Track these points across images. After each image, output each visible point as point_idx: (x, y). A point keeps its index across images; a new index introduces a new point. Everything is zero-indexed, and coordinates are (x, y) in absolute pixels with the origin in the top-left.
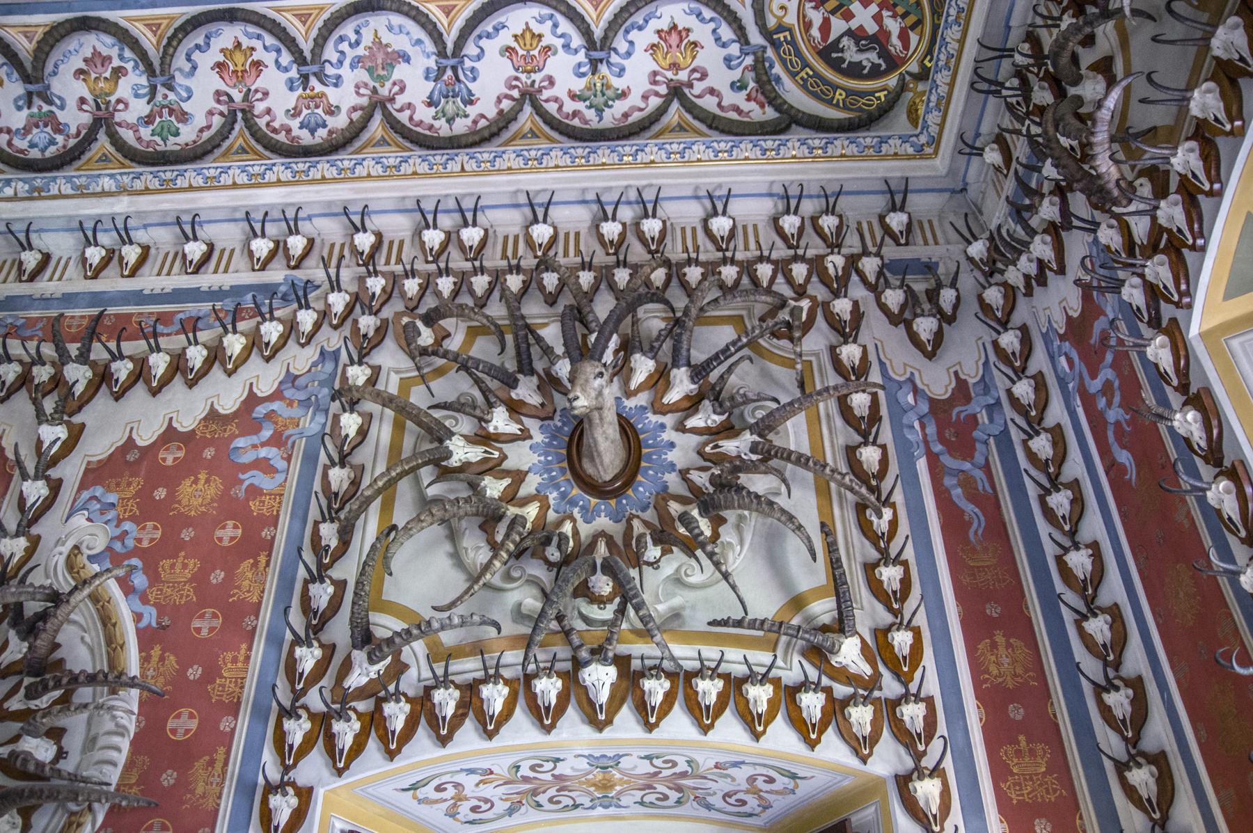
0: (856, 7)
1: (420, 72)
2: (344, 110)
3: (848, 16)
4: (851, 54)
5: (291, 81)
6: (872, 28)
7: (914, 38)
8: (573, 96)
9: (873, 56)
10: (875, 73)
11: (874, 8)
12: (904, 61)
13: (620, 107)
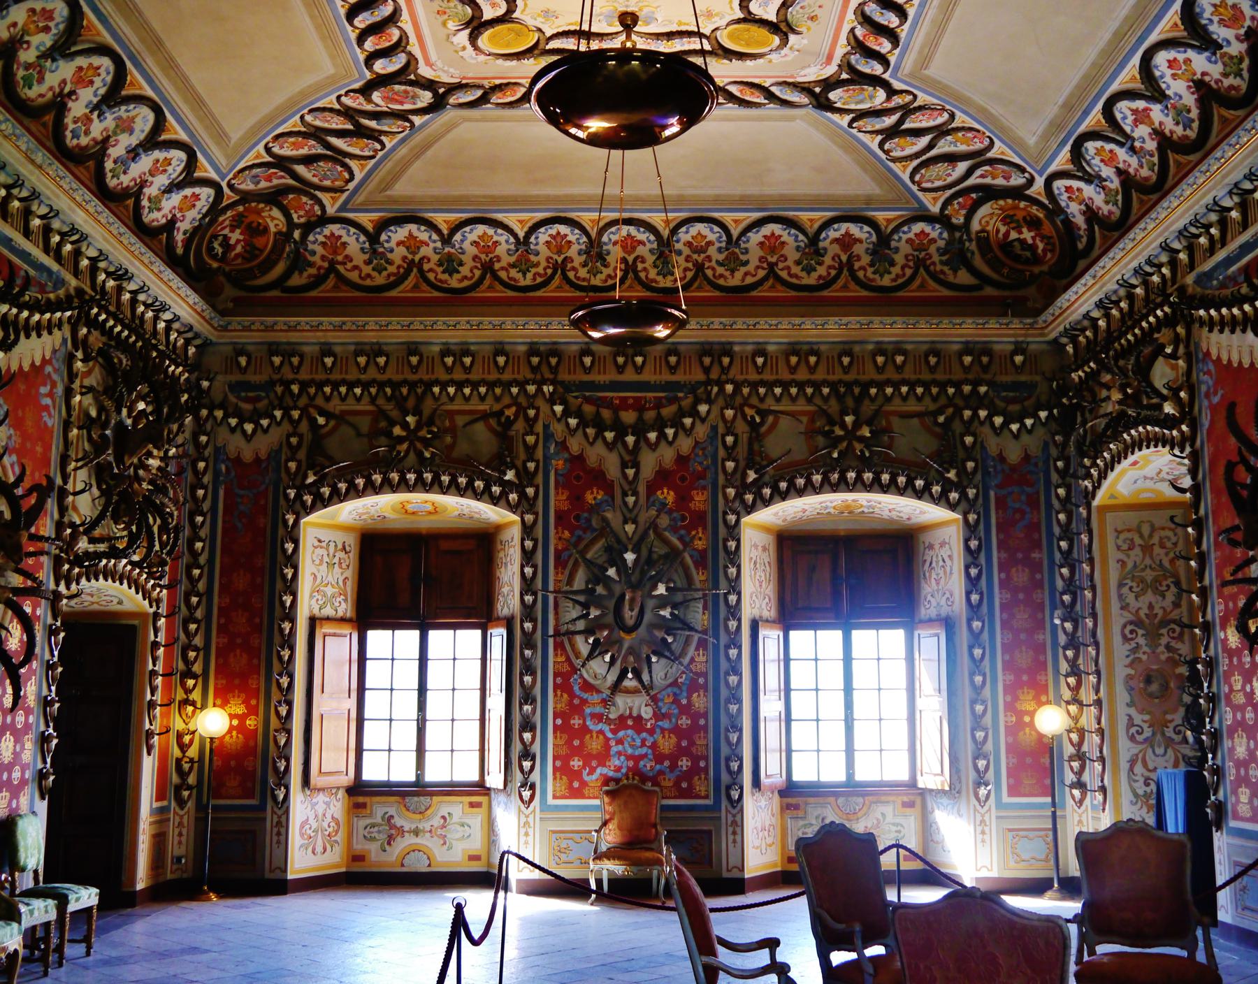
0: (238, 231)
1: (127, 144)
2: (92, 135)
3: (232, 231)
4: (216, 245)
5: (91, 102)
6: (232, 242)
7: (239, 261)
8: (149, 199)
9: (220, 251)
10: (214, 257)
11: (241, 237)
12: (228, 264)
13: (156, 215)
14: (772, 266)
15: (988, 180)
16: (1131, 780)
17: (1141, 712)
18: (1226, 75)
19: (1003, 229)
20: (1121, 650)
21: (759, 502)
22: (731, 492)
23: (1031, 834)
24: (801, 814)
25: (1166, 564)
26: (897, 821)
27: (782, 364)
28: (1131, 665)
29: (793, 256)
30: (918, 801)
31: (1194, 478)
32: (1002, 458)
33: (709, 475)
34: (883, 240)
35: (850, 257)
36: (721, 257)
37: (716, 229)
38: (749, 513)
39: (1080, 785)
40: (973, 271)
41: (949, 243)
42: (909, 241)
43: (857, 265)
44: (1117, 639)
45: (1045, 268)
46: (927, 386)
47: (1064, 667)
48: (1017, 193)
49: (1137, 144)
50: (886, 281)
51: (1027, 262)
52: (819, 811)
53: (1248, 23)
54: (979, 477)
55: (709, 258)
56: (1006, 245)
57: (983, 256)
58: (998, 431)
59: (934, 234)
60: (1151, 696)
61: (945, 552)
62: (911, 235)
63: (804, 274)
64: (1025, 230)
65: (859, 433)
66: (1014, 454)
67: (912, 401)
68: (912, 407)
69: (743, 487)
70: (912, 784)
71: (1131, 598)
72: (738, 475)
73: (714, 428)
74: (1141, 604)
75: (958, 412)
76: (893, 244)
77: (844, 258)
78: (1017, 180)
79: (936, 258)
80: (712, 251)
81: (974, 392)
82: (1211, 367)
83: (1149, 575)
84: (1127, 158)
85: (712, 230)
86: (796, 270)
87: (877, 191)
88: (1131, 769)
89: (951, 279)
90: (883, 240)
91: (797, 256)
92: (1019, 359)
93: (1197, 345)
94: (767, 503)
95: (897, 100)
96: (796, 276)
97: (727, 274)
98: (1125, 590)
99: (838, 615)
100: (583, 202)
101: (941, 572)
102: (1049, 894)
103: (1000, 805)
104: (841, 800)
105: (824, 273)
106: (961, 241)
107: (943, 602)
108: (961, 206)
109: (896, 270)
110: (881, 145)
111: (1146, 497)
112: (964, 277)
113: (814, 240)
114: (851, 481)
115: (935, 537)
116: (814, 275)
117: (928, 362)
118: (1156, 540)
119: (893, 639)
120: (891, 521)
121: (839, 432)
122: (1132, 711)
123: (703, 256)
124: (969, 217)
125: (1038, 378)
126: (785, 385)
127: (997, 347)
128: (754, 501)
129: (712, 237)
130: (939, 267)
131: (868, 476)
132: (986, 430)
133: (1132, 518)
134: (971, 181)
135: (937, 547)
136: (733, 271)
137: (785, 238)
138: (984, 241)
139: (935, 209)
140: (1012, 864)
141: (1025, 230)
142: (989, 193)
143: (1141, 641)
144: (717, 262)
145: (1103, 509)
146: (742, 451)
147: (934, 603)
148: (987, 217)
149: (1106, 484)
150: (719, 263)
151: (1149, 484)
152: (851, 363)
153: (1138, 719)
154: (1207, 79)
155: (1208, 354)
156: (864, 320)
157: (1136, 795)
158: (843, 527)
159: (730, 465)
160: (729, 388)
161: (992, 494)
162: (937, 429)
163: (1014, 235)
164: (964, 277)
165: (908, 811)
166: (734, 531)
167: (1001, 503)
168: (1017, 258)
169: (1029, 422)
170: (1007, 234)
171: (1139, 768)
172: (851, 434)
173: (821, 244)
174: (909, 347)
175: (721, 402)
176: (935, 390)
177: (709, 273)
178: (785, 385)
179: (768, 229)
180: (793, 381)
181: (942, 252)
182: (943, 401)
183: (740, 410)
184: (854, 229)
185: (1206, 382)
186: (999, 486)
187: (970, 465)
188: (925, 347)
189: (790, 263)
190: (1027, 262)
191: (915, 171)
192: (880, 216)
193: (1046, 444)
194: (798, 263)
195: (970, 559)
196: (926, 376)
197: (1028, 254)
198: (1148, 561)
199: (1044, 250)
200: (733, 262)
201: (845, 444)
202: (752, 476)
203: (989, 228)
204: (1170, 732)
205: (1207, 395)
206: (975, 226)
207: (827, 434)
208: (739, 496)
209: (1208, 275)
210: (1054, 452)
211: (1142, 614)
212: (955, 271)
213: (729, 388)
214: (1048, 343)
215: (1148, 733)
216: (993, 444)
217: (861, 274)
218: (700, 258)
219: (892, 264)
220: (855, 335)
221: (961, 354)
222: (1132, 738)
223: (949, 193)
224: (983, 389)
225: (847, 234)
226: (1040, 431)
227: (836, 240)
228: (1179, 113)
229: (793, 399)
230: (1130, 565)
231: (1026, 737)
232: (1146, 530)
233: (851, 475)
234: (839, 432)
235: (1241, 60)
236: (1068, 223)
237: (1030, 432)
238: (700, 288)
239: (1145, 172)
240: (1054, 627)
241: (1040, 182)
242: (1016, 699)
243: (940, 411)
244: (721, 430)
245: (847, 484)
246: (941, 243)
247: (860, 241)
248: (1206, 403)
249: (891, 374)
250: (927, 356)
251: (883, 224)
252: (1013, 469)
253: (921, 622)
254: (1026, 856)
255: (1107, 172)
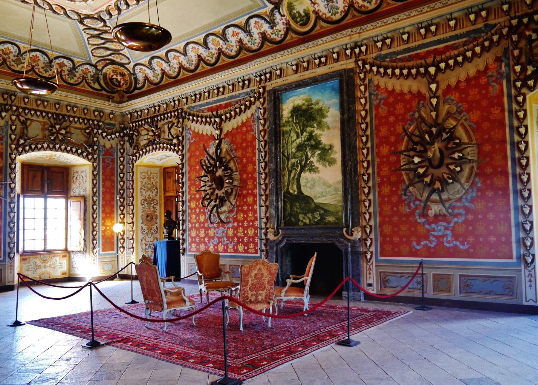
14: (33, 66)
15: (114, 59)
16: (141, 245)
17: (145, 225)
18: (208, 56)
19: (112, 74)
20: (140, 207)
21: (23, 152)
22: (13, 146)
23: (108, 263)
24: (27, 261)
25: (154, 183)
26: (61, 262)
27: (34, 103)
28: (143, 212)
29: (41, 64)
30: (68, 255)
31: (182, 161)
32: (104, 146)
33: (5, 139)
34: (74, 68)
35: (61, 70)
36: (14, 58)
37: (16, 48)
38: (20, 155)
39: (123, 247)
40: (100, 85)
41: (95, 74)
42: (82, 70)
43: (63, 74)
44: (139, 204)
45: (122, 89)
46: (84, 119)
47: (119, 212)
48: (122, 65)
49: (171, 64)
50: (72, 81)
51: (117, 86)
52: (34, 260)
53: (220, 46)
54: (97, 152)
55: (9, 58)
56: (111, 79)
57: (104, 80)
58: (103, 138)
59: (91, 70)
60: (148, 221)
61: (83, 175)
62: (83, 69)
63: (44, 72)
64: (119, 76)
65: (61, 132)
66: (108, 146)
67: (78, 123)
68: (78, 125)
69: (18, 145)
70: (66, 250)
71: (144, 193)
72: (16, 140)
73: (7, 122)
74: (147, 194)
75: (93, 130)
76: (77, 70)
77: (59, 70)
78: (125, 61)
79: (89, 78)
80: (11, 55)
81: (98, 124)
82: (191, 132)
83: (149, 186)
84: (166, 67)
85: (13, 48)
86: (42, 70)
87: (78, 52)
88: (142, 242)
89: (93, 85)
90: (74, 68)
91: (43, 65)
92: (111, 116)
93: (186, 126)
94: (27, 152)
95: (105, 28)
96: (41, 72)
97: (15, 65)
98: (142, 190)
99: (43, 193)
100: (21, 39)
101: (81, 181)
102: (116, 279)
103: (99, 255)
104: (42, 256)
105: (51, 74)
106: (98, 74)
107: (82, 190)
108: (102, 64)
109: (76, 79)
110: (88, 39)
111: (151, 164)
112: (97, 86)
113: (51, 61)
114: (63, 149)
115: (79, 169)
116: (48, 74)
117: (55, 107)
118: (151, 176)
119: (60, 202)
120: (63, 162)
121: (54, 131)
122: (143, 225)
123: (7, 56)
124: (103, 68)
125: (116, 123)
126: (36, 111)
127: (106, 111)
128: (22, 151)
129: (12, 50)
130: (90, 81)
131: (63, 147)
132: (100, 137)
133: (146, 169)
134: (110, 57)
135: (80, 173)
136: (18, 65)
137: (40, 58)
138: (105, 76)
139: (94, 62)
140: (102, 272)
141: (119, 76)
142: (113, 62)
143: (146, 205)
144: (12, 60)
145: (137, 166)
146: (18, 131)
147: (77, 190)
148: (108, 70)
149: (141, 159)
150: (13, 61)
151: (153, 160)
152: (59, 107)
153: (144, 227)
154: (202, 55)
155: (190, 129)
156: (67, 94)
157: (143, 249)
158: (45, 163)
159: (13, 137)
160: (14, 108)
161: (101, 157)
162: (86, 134)
163: (115, 77)
164: (97, 86)
165: (64, 258)
166: (13, 160)
167: (104, 160)
168: (114, 84)
169: (113, 136)
170: (113, 76)
171: (144, 241)
172: (58, 132)
173: (53, 64)
174: (79, 105)
175: (10, 112)
176: (86, 121)
177: (8, 63)
178: (36, 111)
179: (34, 53)
180: (44, 111)
181: (92, 76)
182: (88, 125)
183: (18, 116)
184: (66, 61)
185: (188, 136)
186: (103, 155)
187: (95, 147)
188: (84, 107)
189: (40, 67)
190: (117, 86)
191: (94, 49)
192: (76, 60)
193: (117, 144)
194: (43, 68)
195: (94, 178)
196: (83, 116)
197: (118, 83)
198: (149, 182)
199: (123, 84)
200: (18, 61)
201: (55, 135)
202: (22, 141)
203: (108, 73)
204: (152, 231)
205: (189, 139)
206: (104, 71)
207: (50, 131)
208: (16, 149)
209: (193, 107)
210: (119, 147)
211: (147, 197)
212: (94, 83)
213: (14, 108)
214: (121, 112)
215: (147, 231)
216: (102, 141)
217: (64, 77)
218: (6, 57)
219: (75, 76)
220: (62, 98)
221: (94, 111)
222: (142, 233)
223: (101, 58)
224: (101, 124)
225: (63, 62)
226: (116, 139)
227: (58, 64)
228: (189, 61)
229: (38, 116)
230: (144, 183)
231: (108, 233)
232: (149, 173)
233: (57, 146)
234: (54, 131)
235: (214, 54)
236: (136, 79)
237: (113, 139)
238: (3, 68)
239: (171, 72)
240: (117, 200)
241: (132, 64)
242: (105, 222)
243: (87, 128)
244: (10, 123)
245: (56, 149)
246: (92, 74)
247: (66, 66)
248: (188, 142)
249: (71, 113)
250: (55, 104)
251: (76, 62)
252: (108, 150)
253: (71, 197)
254: (106, 269)
255: (157, 68)
